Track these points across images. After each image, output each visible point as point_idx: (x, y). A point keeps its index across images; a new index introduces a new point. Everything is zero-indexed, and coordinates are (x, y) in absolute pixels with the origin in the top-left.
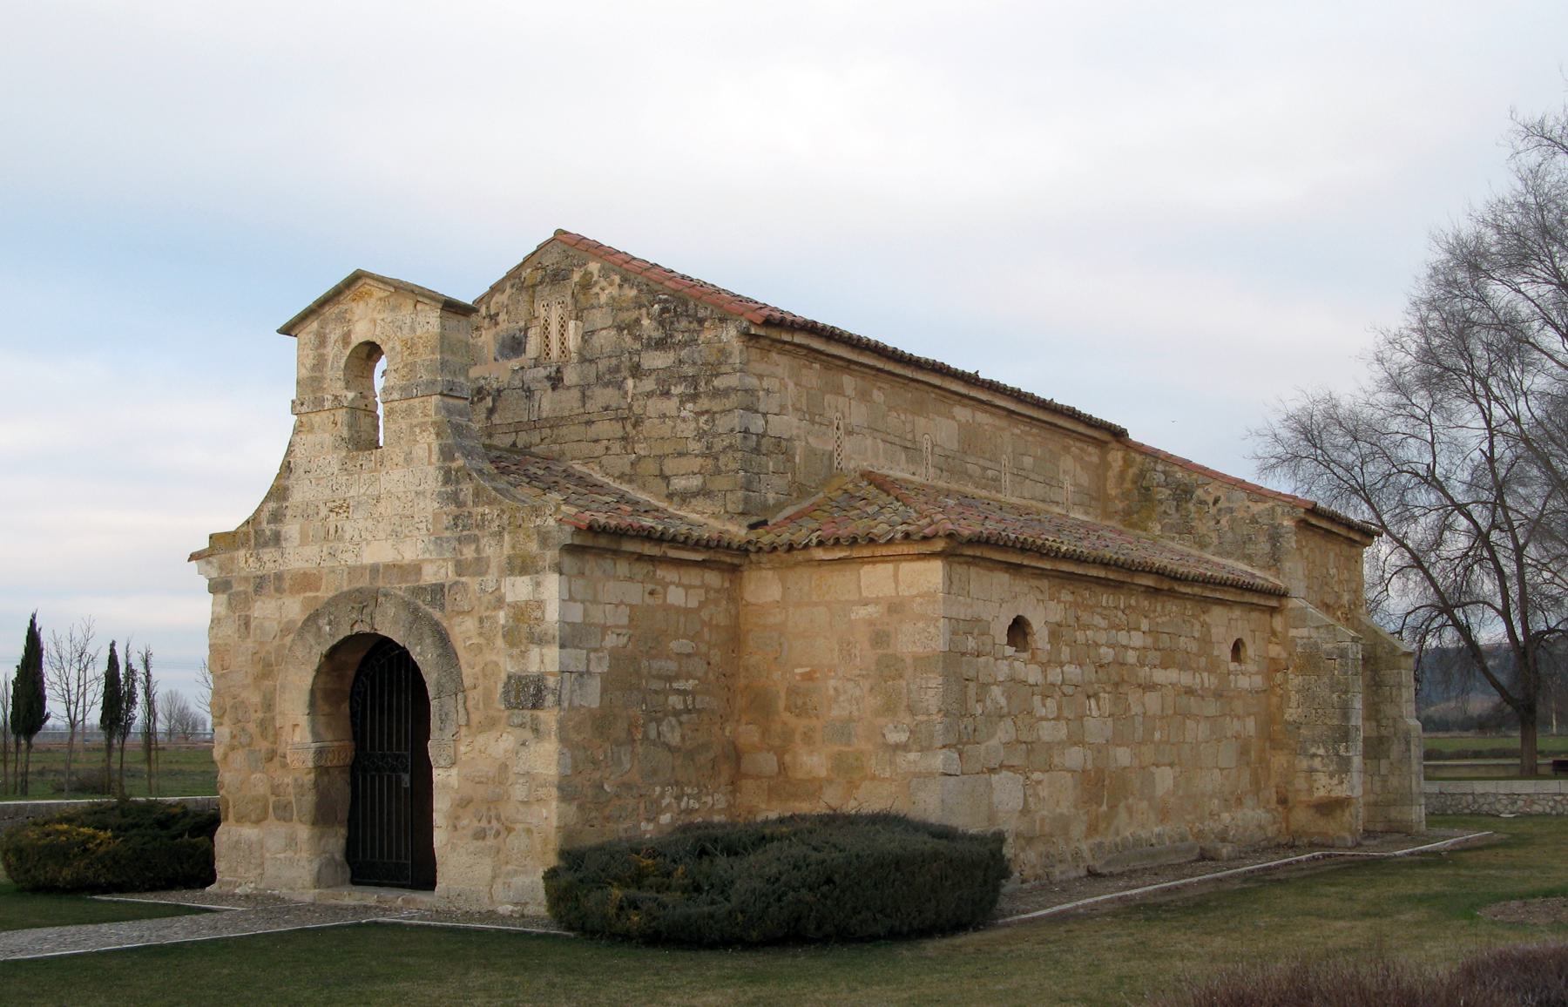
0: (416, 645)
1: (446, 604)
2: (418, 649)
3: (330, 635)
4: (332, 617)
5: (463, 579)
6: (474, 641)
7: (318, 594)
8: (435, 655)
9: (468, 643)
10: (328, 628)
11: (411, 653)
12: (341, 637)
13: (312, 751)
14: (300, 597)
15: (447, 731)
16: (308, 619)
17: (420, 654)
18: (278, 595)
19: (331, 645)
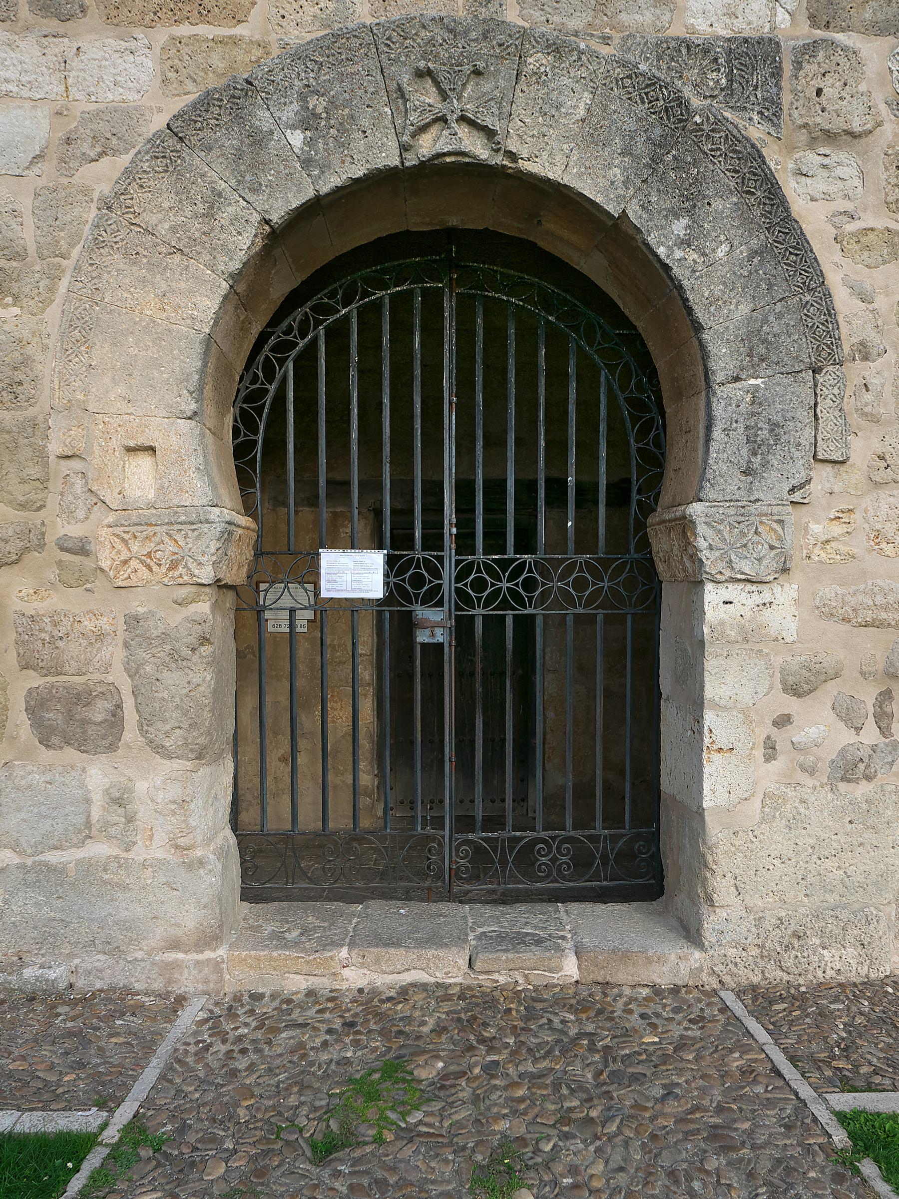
0: (675, 214)
1: (786, 98)
2: (679, 227)
3: (307, 163)
4: (318, 104)
5: (840, 37)
6: (868, 221)
7: (239, 30)
8: (742, 252)
9: (851, 227)
10: (297, 138)
11: (651, 239)
12: (359, 172)
13: (212, 532)
14: (162, 34)
15: (772, 476)
16: (206, 102)
17: (685, 243)
18: (54, 25)
19: (310, 194)
